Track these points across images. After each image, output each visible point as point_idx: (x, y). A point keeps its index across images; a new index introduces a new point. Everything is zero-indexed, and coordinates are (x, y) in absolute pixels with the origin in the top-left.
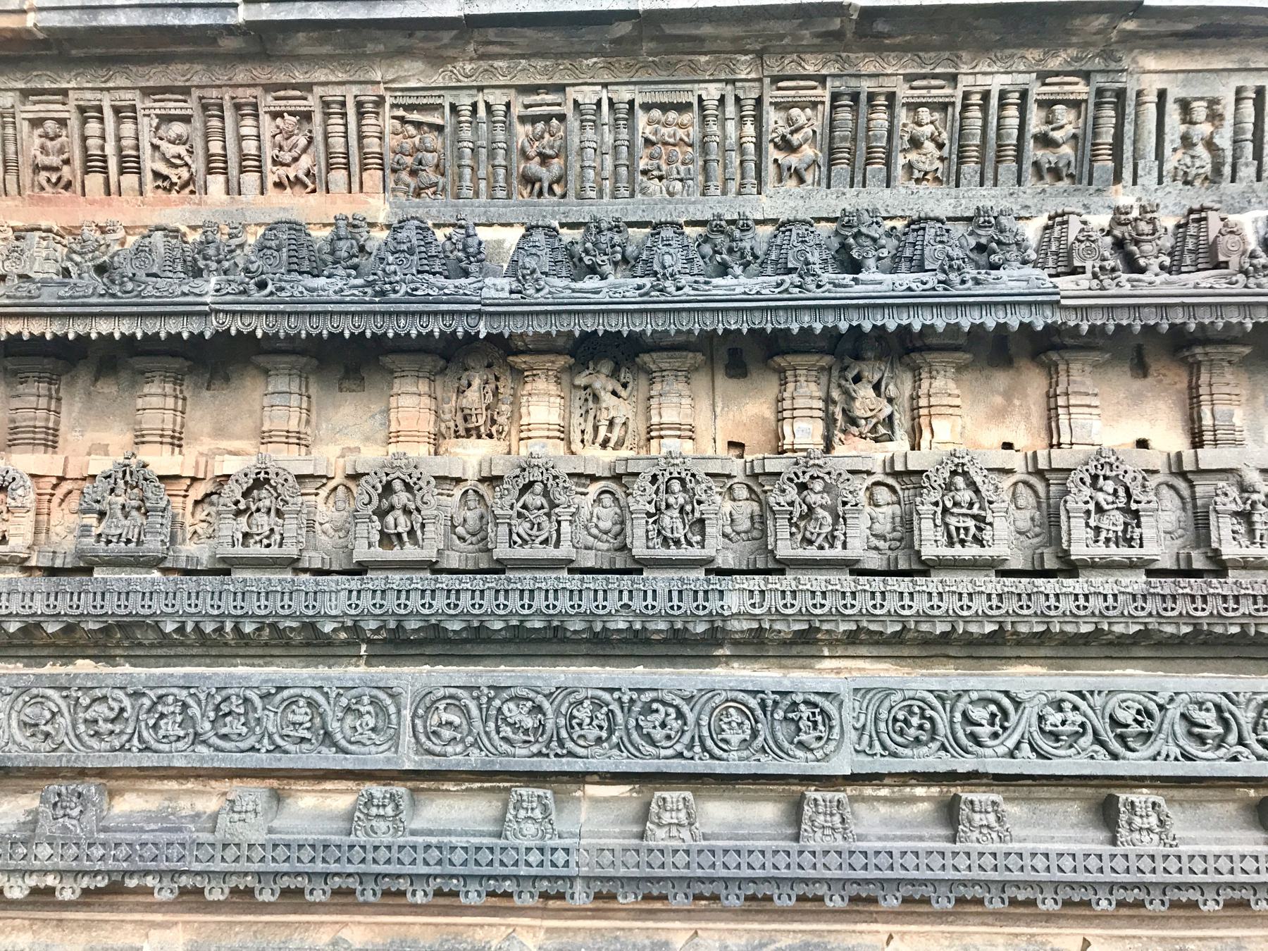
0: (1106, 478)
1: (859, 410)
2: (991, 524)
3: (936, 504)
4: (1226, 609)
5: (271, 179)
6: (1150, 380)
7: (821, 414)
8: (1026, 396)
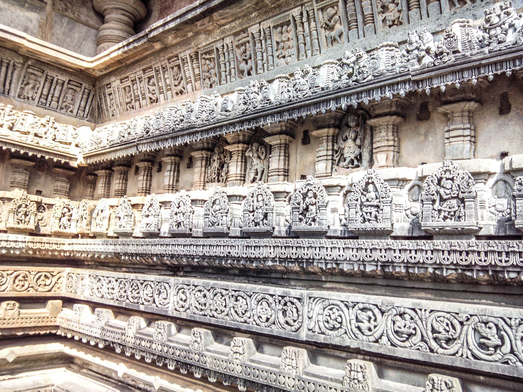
0: (447, 179)
2: (382, 210)
4: (501, 261)
6: (512, 114)
8: (436, 134)
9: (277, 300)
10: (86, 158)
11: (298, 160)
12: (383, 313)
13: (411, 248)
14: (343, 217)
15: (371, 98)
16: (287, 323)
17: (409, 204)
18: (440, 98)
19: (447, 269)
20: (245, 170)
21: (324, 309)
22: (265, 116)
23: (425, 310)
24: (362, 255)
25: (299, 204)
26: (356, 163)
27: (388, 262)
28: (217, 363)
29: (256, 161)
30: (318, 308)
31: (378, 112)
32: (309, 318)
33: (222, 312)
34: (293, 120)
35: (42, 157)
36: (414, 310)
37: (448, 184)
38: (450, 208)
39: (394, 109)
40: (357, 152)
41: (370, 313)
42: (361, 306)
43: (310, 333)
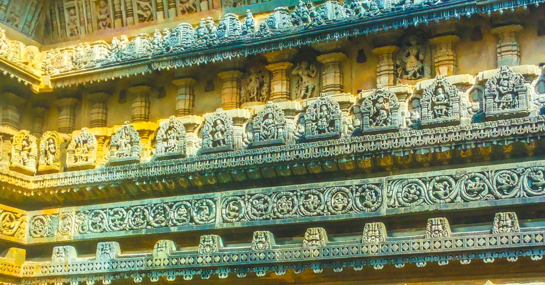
1: (408, 69)
3: (429, 101)
5: (180, 9)
7: (392, 72)
9: (354, 189)
10: (54, 81)
11: (354, 77)
12: (456, 180)
13: (480, 128)
14: (409, 120)
15: (442, 18)
16: (366, 206)
17: (470, 104)
18: (495, 21)
19: (508, 140)
20: (290, 89)
21: (403, 187)
22: (332, 33)
23: (491, 171)
24: (438, 139)
25: (369, 109)
26: (418, 75)
27: (460, 142)
28: (288, 254)
29: (305, 79)
30: (396, 188)
31: (439, 32)
32: (388, 197)
33: (289, 212)
34: (364, 35)
35: (8, 75)
36: (482, 173)
37: (505, 83)
38: (507, 100)
39: (453, 30)
40: (420, 66)
41: (446, 183)
42: (438, 178)
43: (391, 208)
